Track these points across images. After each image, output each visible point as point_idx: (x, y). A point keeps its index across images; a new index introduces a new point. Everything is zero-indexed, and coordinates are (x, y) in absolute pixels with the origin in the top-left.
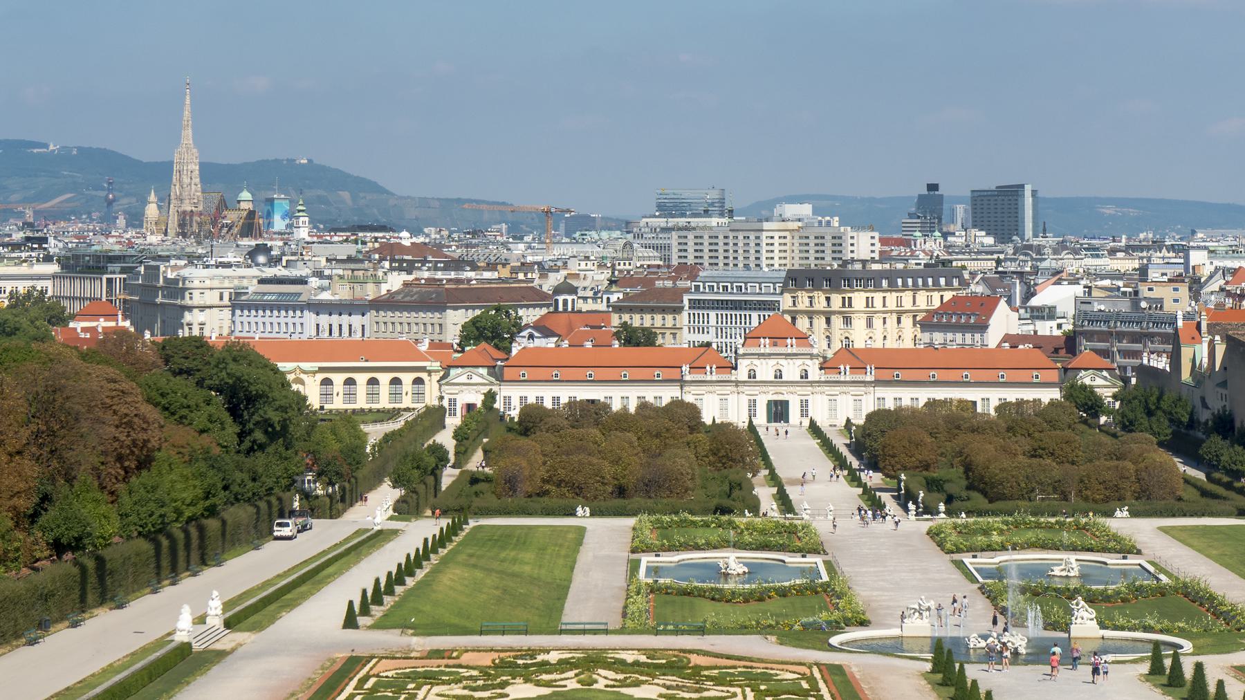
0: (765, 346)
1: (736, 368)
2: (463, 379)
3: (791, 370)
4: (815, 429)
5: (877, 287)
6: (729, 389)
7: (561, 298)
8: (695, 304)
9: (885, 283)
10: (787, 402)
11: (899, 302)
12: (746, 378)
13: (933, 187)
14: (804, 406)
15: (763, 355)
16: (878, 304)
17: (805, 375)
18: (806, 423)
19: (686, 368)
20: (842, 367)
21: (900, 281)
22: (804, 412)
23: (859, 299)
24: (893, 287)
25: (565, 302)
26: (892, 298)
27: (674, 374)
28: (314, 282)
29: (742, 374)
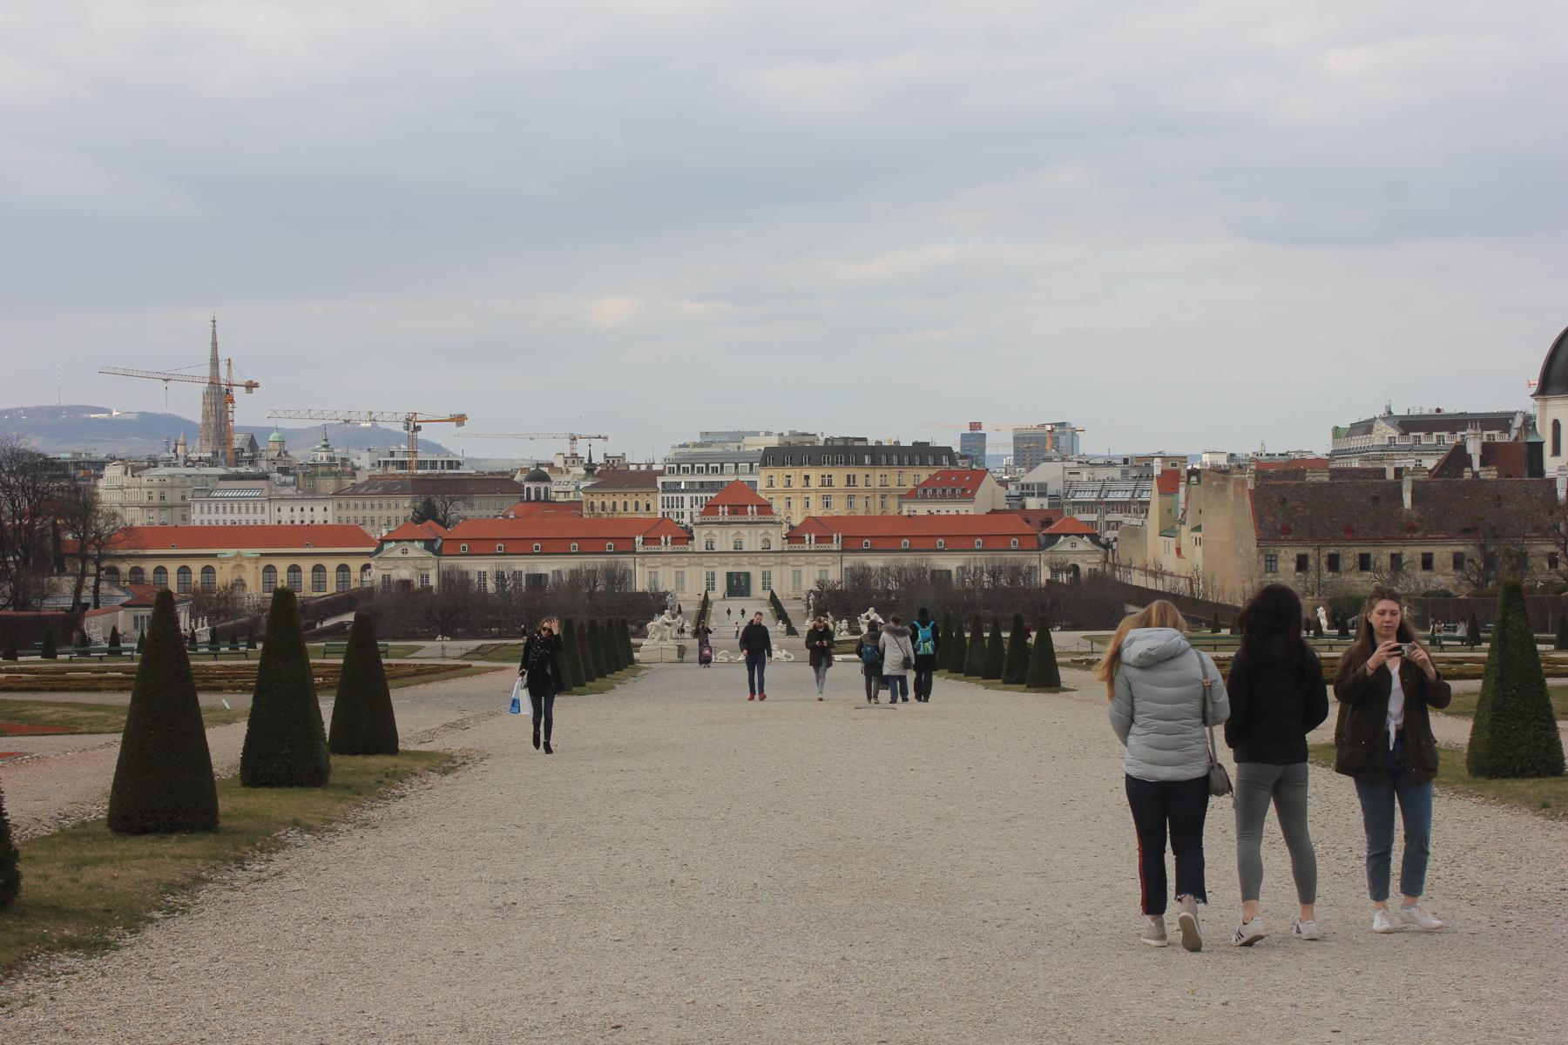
0: (723, 513)
1: (692, 538)
2: (398, 553)
3: (752, 539)
4: (774, 600)
5: (859, 463)
6: (686, 559)
7: (532, 486)
8: (667, 487)
9: (867, 459)
10: (747, 575)
13: (975, 426)
14: (766, 578)
16: (860, 481)
18: (767, 595)
19: (639, 539)
21: (884, 458)
22: (766, 585)
23: (839, 475)
24: (874, 463)
25: (538, 492)
26: (876, 475)
28: (276, 475)
29: (699, 543)
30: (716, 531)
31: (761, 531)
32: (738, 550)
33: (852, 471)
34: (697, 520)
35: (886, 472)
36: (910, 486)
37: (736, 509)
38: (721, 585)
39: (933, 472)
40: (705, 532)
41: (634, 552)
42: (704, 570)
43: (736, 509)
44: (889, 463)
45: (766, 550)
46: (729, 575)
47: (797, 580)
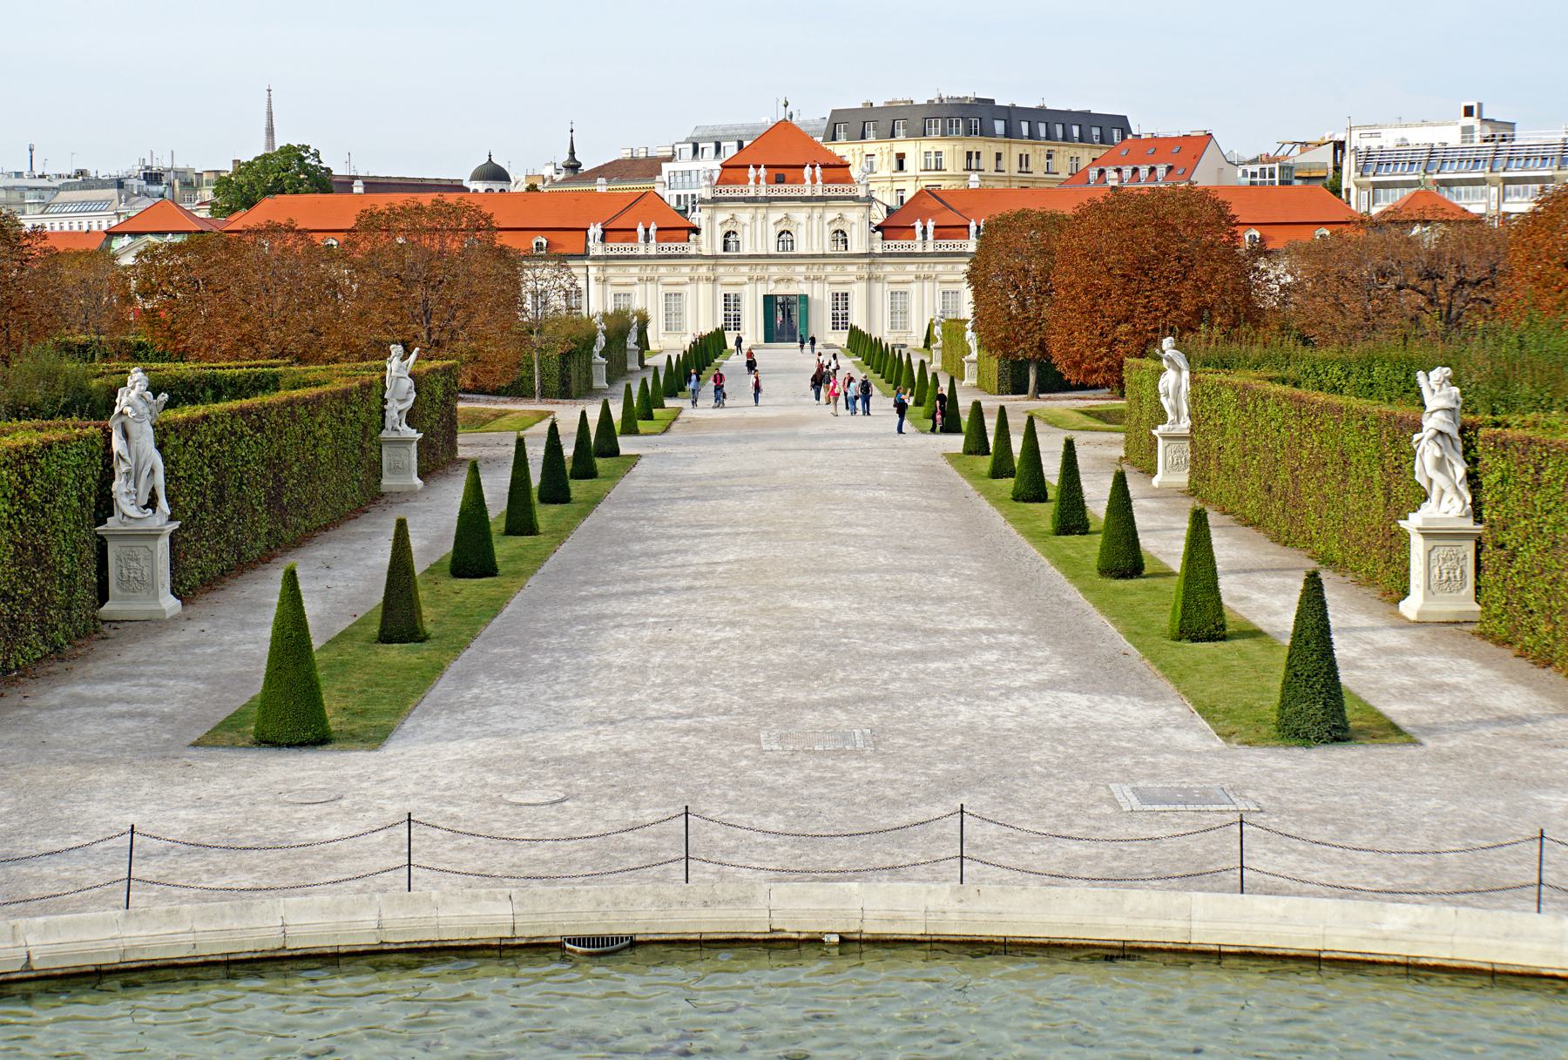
3: (812, 231)
5: (987, 132)
9: (999, 126)
10: (804, 299)
11: (1024, 160)
12: (719, 251)
14: (842, 299)
15: (754, 200)
16: (988, 162)
17: (841, 236)
18: (842, 338)
19: (595, 231)
20: (918, 225)
22: (840, 320)
24: (1009, 133)
29: (709, 242)
30: (745, 215)
32: (786, 253)
33: (974, 145)
34: (706, 194)
35: (1028, 149)
36: (1064, 175)
39: (1098, 154)
40: (722, 216)
44: (1032, 135)
46: (769, 300)
47: (899, 313)
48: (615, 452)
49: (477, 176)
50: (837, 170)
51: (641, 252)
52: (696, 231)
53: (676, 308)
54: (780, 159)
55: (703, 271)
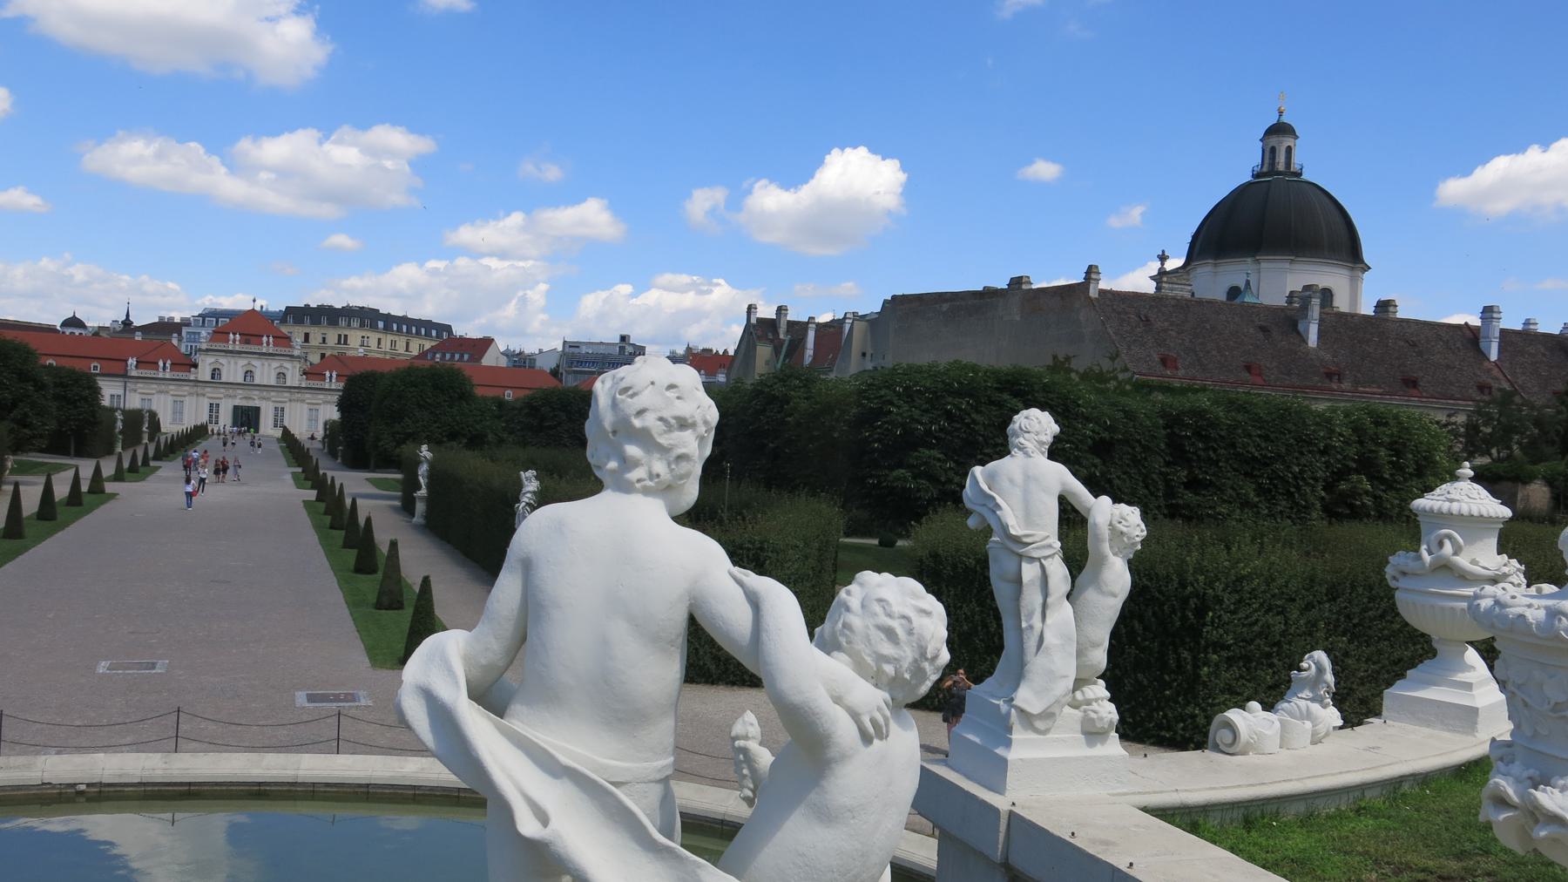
1: (196, 366)
3: (265, 372)
5: (374, 327)
10: (258, 409)
11: (393, 343)
12: (208, 378)
14: (279, 413)
18: (278, 433)
19: (132, 362)
24: (387, 329)
26: (387, 340)
27: (115, 367)
29: (204, 373)
31: (275, 364)
32: (248, 381)
34: (204, 346)
36: (415, 353)
37: (250, 337)
38: (225, 419)
40: (212, 360)
41: (124, 375)
42: (205, 403)
43: (250, 337)
45: (281, 386)
48: (102, 491)
49: (66, 323)
50: (284, 340)
51: (161, 375)
52: (196, 366)
53: (176, 409)
54: (248, 329)
55: (200, 390)
